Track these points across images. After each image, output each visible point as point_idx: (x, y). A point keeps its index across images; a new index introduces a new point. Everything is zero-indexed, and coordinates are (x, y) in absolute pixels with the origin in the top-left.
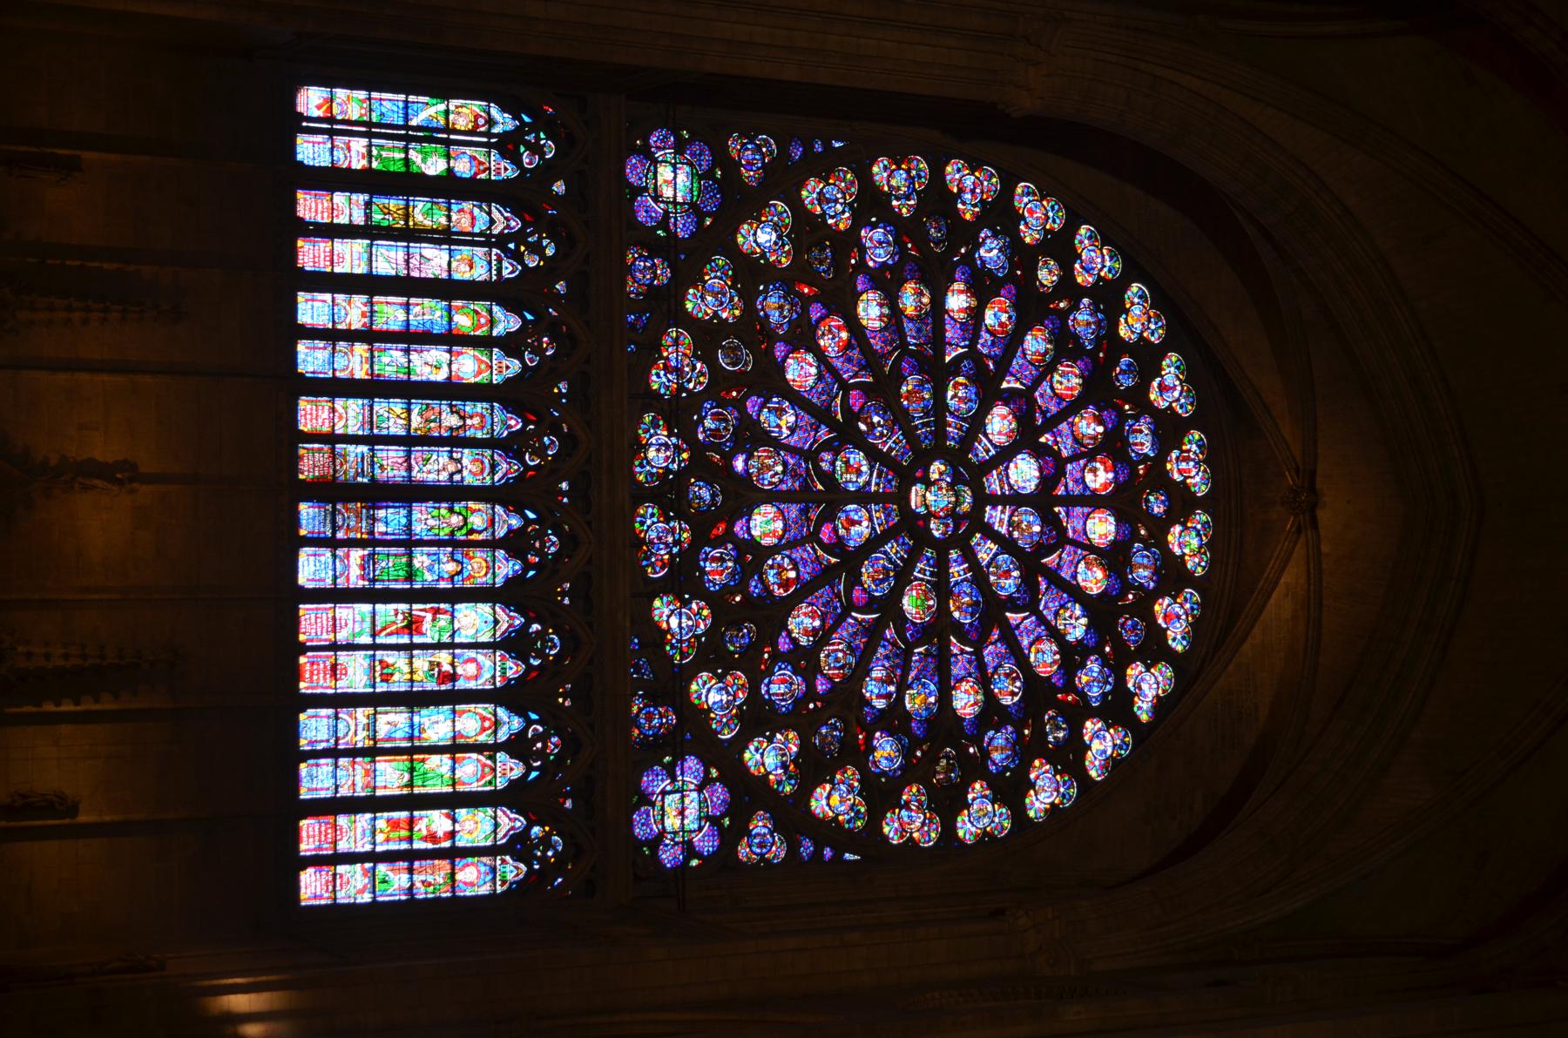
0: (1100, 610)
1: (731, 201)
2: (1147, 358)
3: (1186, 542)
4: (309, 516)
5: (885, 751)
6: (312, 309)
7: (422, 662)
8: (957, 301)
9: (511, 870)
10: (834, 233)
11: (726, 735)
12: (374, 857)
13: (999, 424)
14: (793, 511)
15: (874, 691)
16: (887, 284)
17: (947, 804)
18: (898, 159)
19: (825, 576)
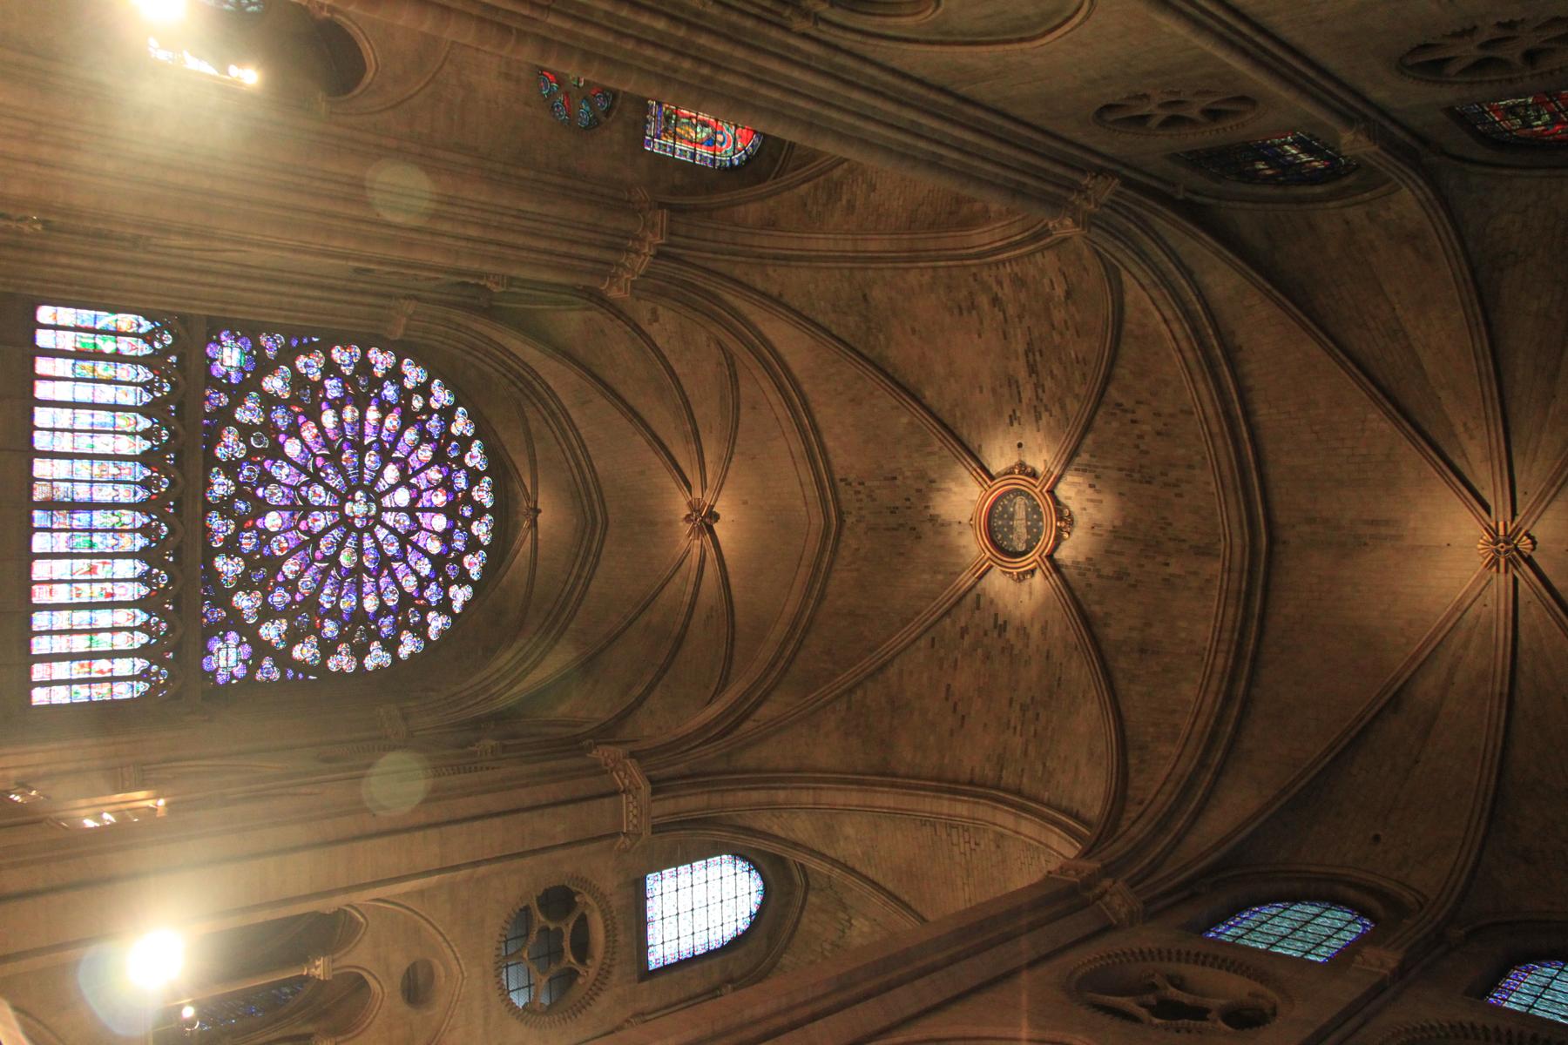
0: (438, 562)
1: (261, 366)
2: (465, 443)
3: (481, 529)
4: (39, 517)
5: (330, 629)
6: (42, 416)
7: (97, 587)
8: (372, 414)
9: (142, 687)
10: (312, 383)
11: (251, 621)
12: (70, 682)
13: (391, 473)
14: (287, 515)
15: (325, 601)
16: (338, 406)
17: (360, 652)
18: (345, 346)
19: (302, 546)
